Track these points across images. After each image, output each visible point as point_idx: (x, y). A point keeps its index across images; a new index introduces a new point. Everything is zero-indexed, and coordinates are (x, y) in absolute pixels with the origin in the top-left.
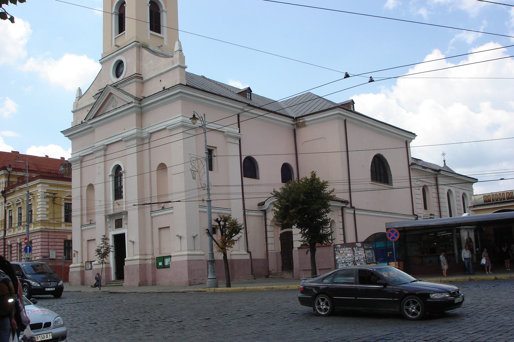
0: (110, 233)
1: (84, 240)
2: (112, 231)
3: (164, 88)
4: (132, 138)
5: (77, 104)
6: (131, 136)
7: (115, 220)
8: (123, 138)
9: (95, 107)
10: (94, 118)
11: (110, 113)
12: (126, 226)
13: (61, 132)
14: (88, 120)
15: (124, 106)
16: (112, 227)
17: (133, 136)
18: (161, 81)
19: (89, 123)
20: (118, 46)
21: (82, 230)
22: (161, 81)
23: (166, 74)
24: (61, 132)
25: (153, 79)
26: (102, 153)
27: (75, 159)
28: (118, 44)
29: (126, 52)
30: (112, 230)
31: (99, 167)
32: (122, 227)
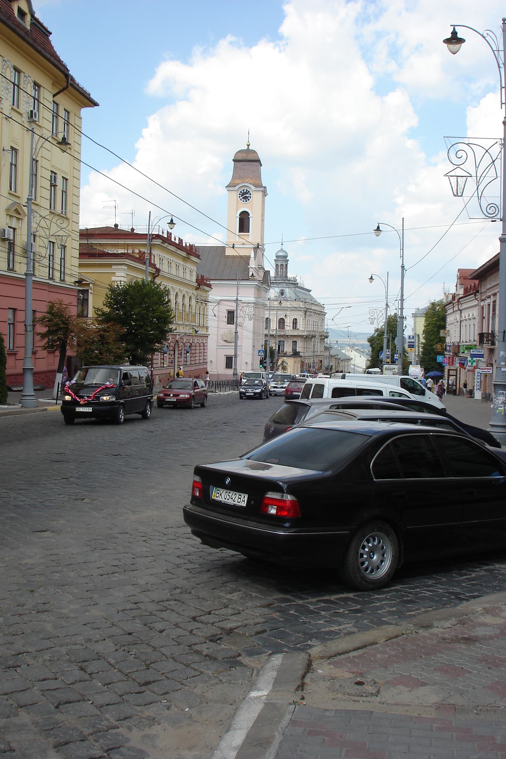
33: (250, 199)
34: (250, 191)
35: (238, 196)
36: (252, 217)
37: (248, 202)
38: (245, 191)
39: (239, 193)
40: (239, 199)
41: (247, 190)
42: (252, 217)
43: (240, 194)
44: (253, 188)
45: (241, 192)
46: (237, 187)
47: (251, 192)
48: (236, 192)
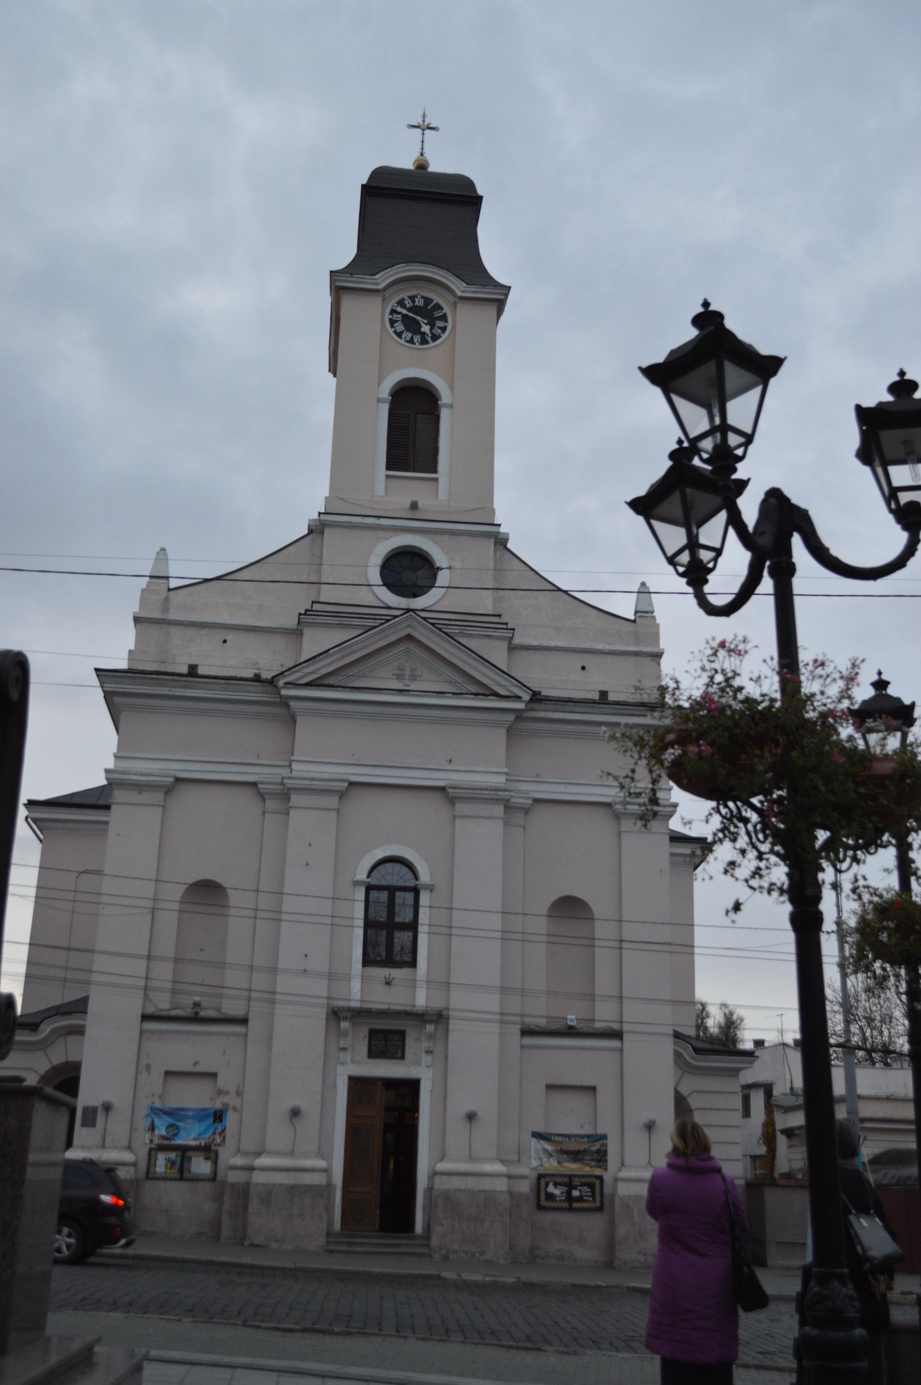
0: (340, 1069)
1: (148, 1068)
2: (352, 1062)
3: (604, 694)
4: (495, 797)
5: (166, 600)
6: (491, 793)
7: (367, 1033)
8: (452, 788)
9: (335, 653)
10: (309, 685)
11: (406, 695)
12: (426, 1059)
13: (97, 670)
14: (286, 683)
15: (480, 697)
16: (350, 1051)
17: (499, 793)
18: (583, 668)
19: (284, 692)
20: (414, 506)
21: (142, 1032)
22: (583, 668)
23: (609, 658)
24: (97, 670)
25: (553, 652)
26: (333, 801)
27: (139, 778)
28: (421, 504)
29: (445, 538)
30: (349, 1060)
31: (310, 845)
32: (403, 1057)
33: (444, 336)
34: (442, 303)
35: (387, 316)
36: (451, 406)
37: (432, 344)
38: (419, 302)
39: (392, 303)
40: (391, 331)
41: (428, 301)
42: (451, 406)
43: (393, 312)
44: (459, 287)
45: (401, 303)
46: (383, 279)
47: (447, 310)
48: (377, 301)
